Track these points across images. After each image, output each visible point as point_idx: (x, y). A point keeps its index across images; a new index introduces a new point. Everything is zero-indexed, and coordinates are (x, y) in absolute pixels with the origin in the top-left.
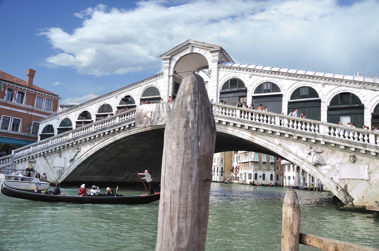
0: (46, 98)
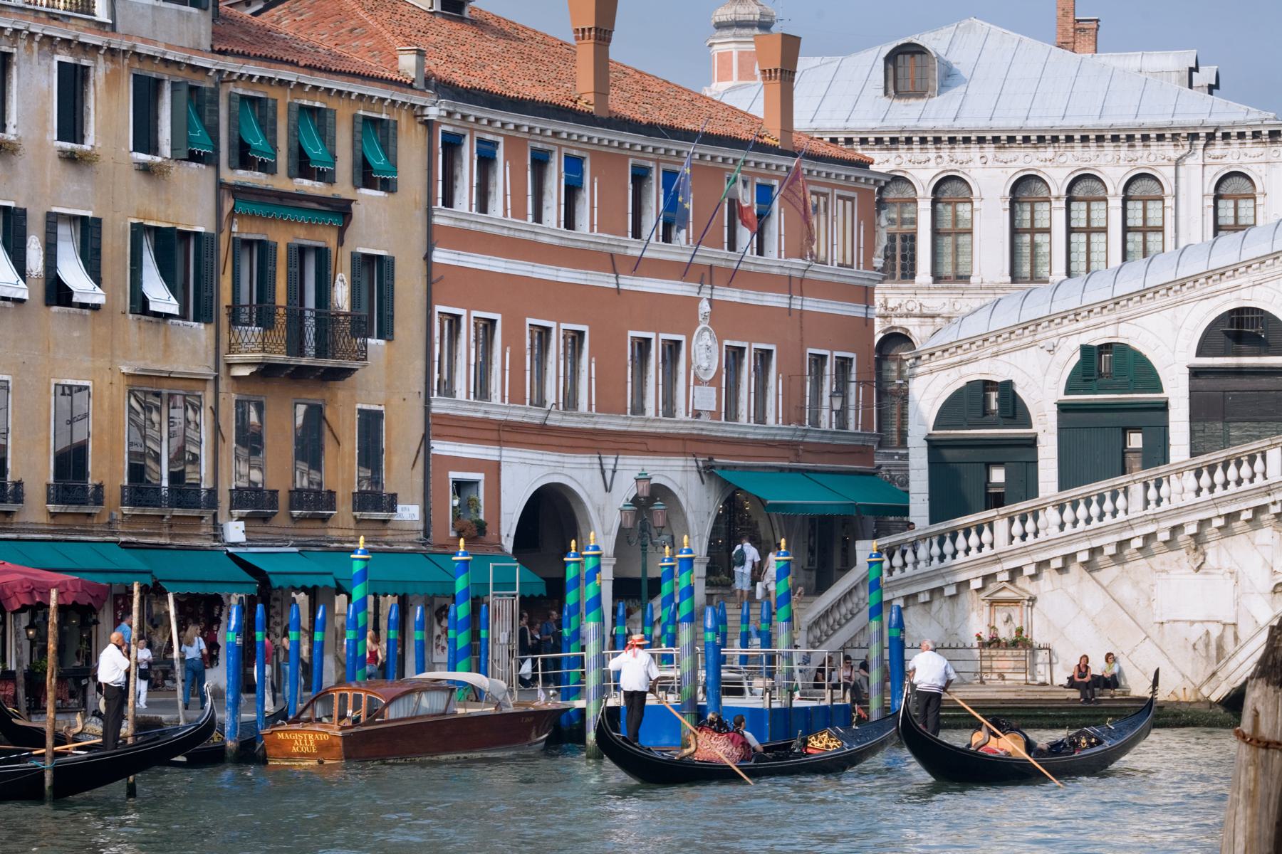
0: (836, 192)
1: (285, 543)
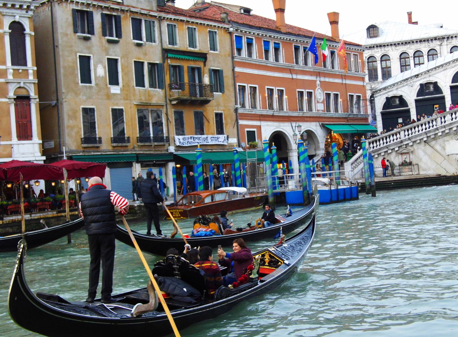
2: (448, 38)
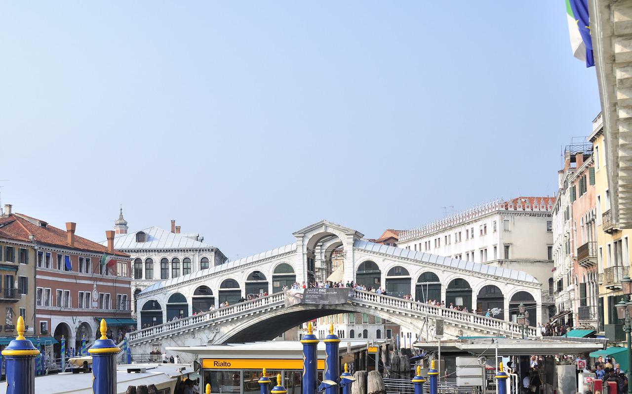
1: (4, 336)
2: (200, 250)
